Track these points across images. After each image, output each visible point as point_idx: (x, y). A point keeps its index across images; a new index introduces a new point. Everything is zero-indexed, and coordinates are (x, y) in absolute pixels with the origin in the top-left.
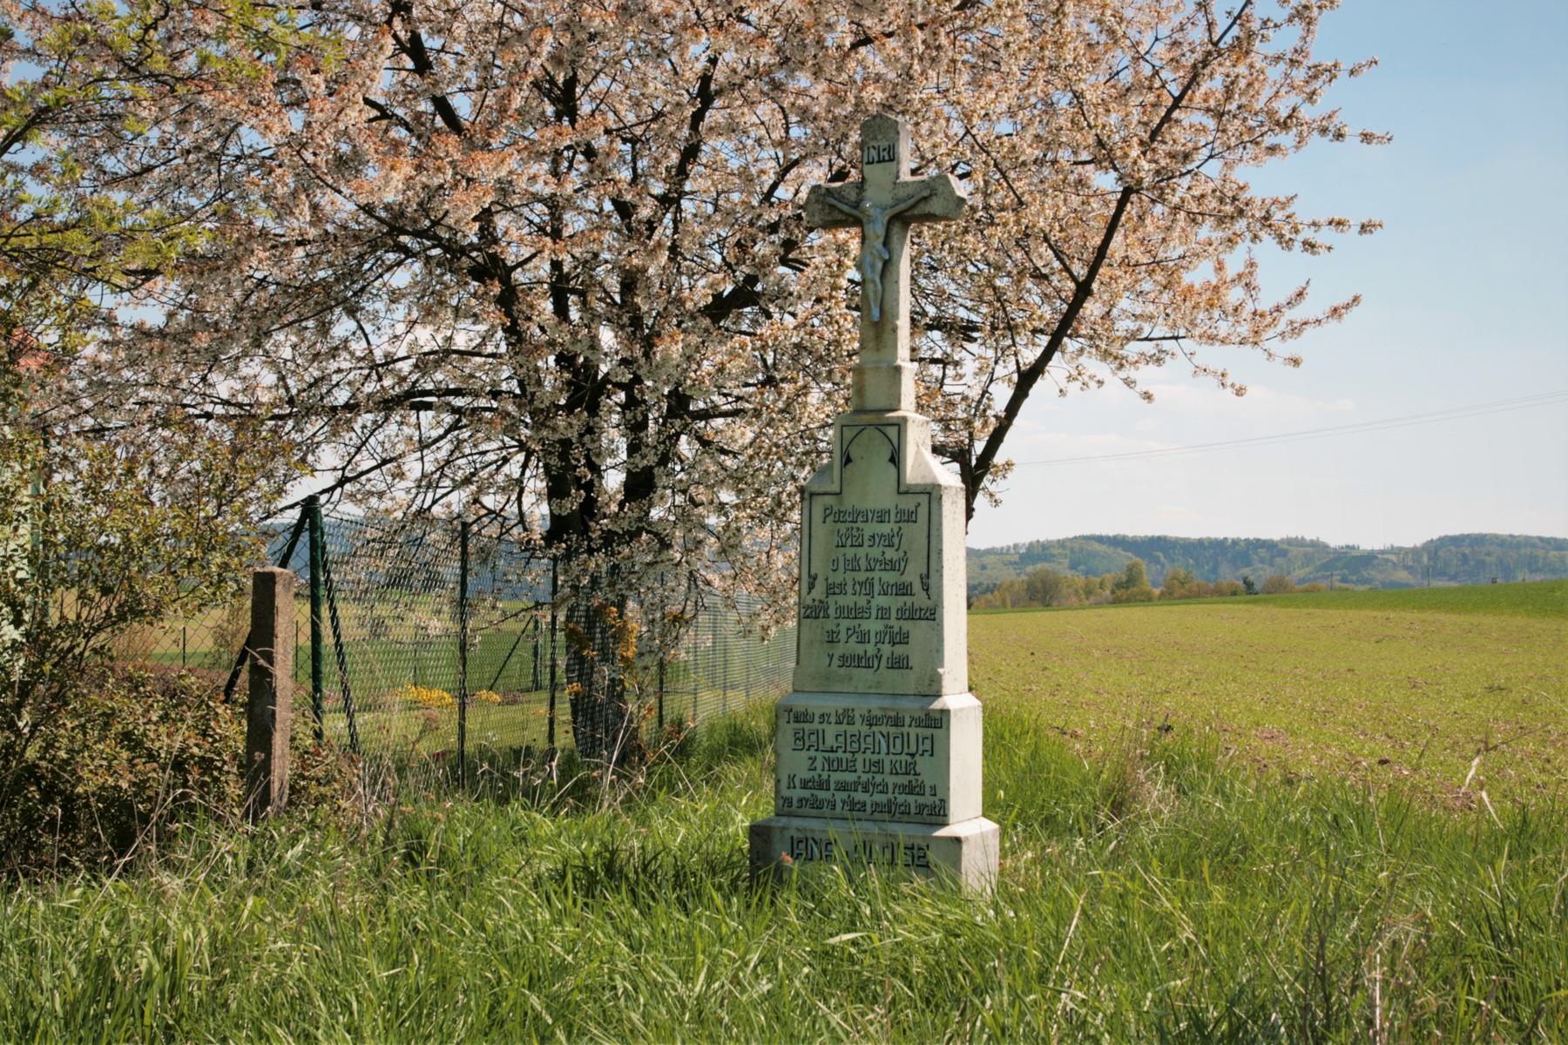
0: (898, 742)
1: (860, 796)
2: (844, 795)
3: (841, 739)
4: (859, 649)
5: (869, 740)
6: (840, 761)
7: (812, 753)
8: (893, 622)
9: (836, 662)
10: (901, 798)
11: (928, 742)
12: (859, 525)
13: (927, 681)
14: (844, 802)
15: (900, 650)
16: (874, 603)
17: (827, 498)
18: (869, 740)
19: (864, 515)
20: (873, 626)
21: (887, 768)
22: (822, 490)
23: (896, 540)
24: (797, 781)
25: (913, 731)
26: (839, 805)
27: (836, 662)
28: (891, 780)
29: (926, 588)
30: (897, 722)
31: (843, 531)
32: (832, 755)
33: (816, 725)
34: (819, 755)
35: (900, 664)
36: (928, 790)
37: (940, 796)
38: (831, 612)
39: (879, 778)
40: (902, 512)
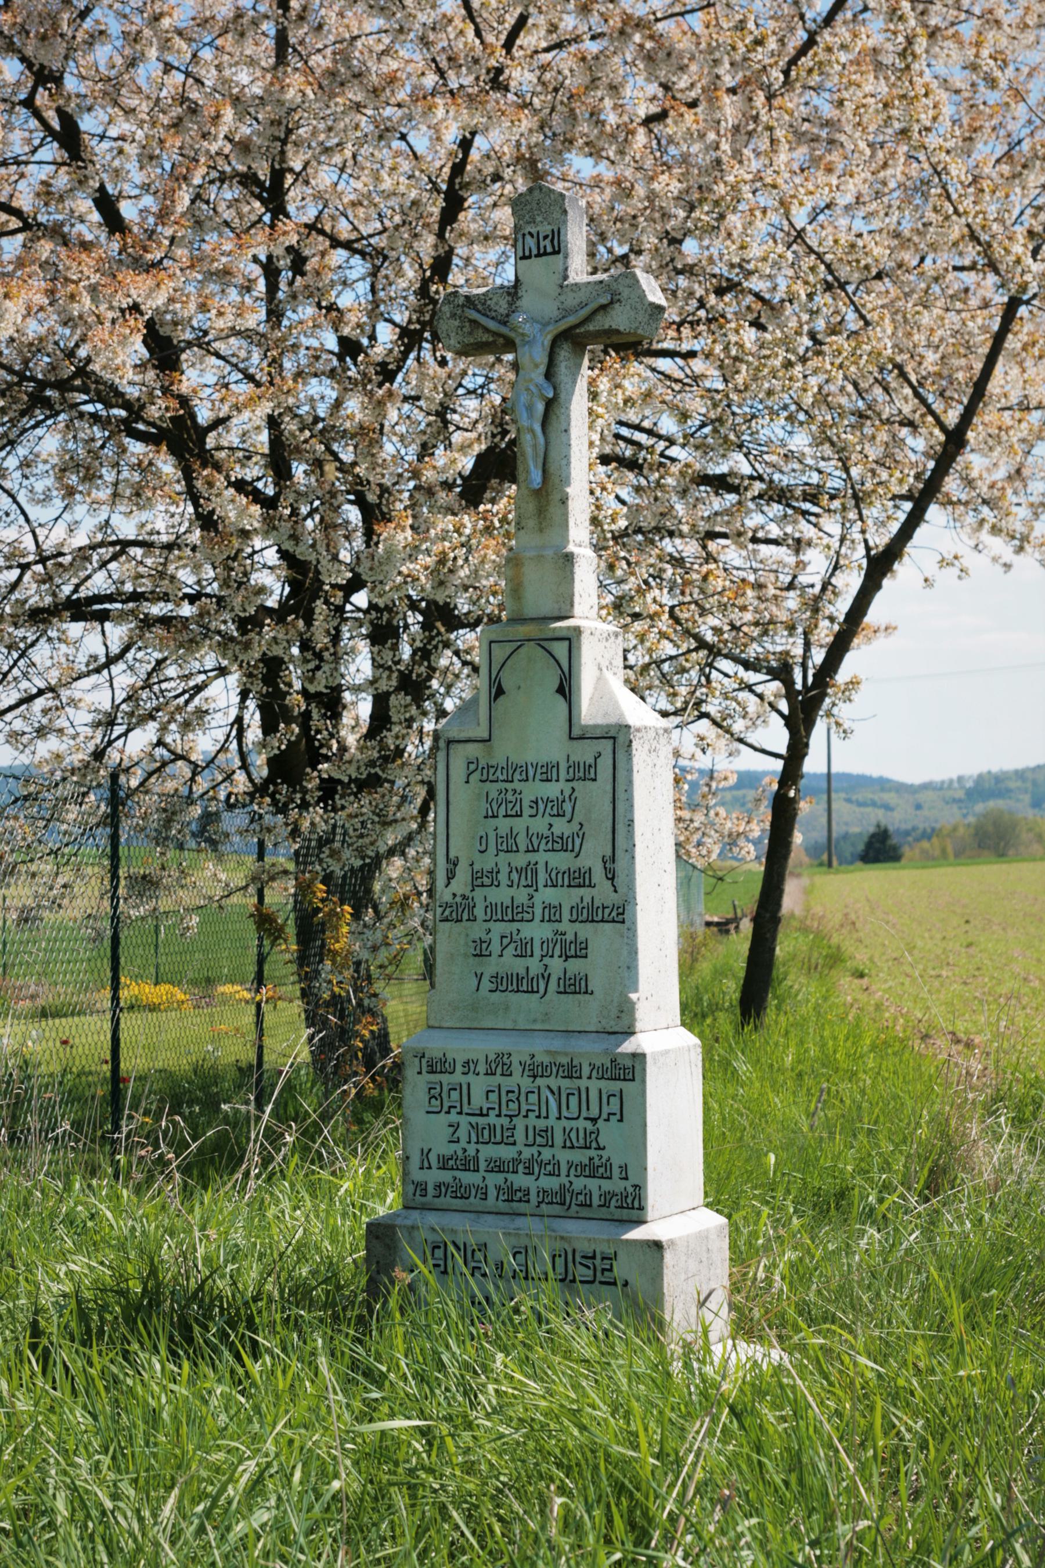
0: (574, 1101)
1: (520, 1180)
2: (498, 1179)
3: (493, 1097)
4: (518, 966)
5: (533, 1098)
6: (492, 1129)
7: (453, 1117)
8: (565, 926)
9: (486, 985)
10: (579, 1183)
11: (615, 1101)
12: (517, 785)
13: (614, 1012)
14: (498, 1189)
15: (575, 966)
16: (538, 899)
17: (470, 746)
18: (533, 1098)
19: (522, 771)
20: (537, 931)
21: (559, 1139)
22: (463, 736)
23: (567, 807)
24: (433, 1158)
25: (594, 1085)
26: (492, 1193)
27: (486, 985)
28: (564, 1157)
29: (611, 877)
30: (571, 1072)
31: (493, 795)
32: (482, 1121)
33: (458, 1077)
34: (464, 1120)
35: (575, 987)
36: (616, 1172)
37: (633, 1180)
38: (479, 912)
39: (547, 1154)
40: (576, 766)
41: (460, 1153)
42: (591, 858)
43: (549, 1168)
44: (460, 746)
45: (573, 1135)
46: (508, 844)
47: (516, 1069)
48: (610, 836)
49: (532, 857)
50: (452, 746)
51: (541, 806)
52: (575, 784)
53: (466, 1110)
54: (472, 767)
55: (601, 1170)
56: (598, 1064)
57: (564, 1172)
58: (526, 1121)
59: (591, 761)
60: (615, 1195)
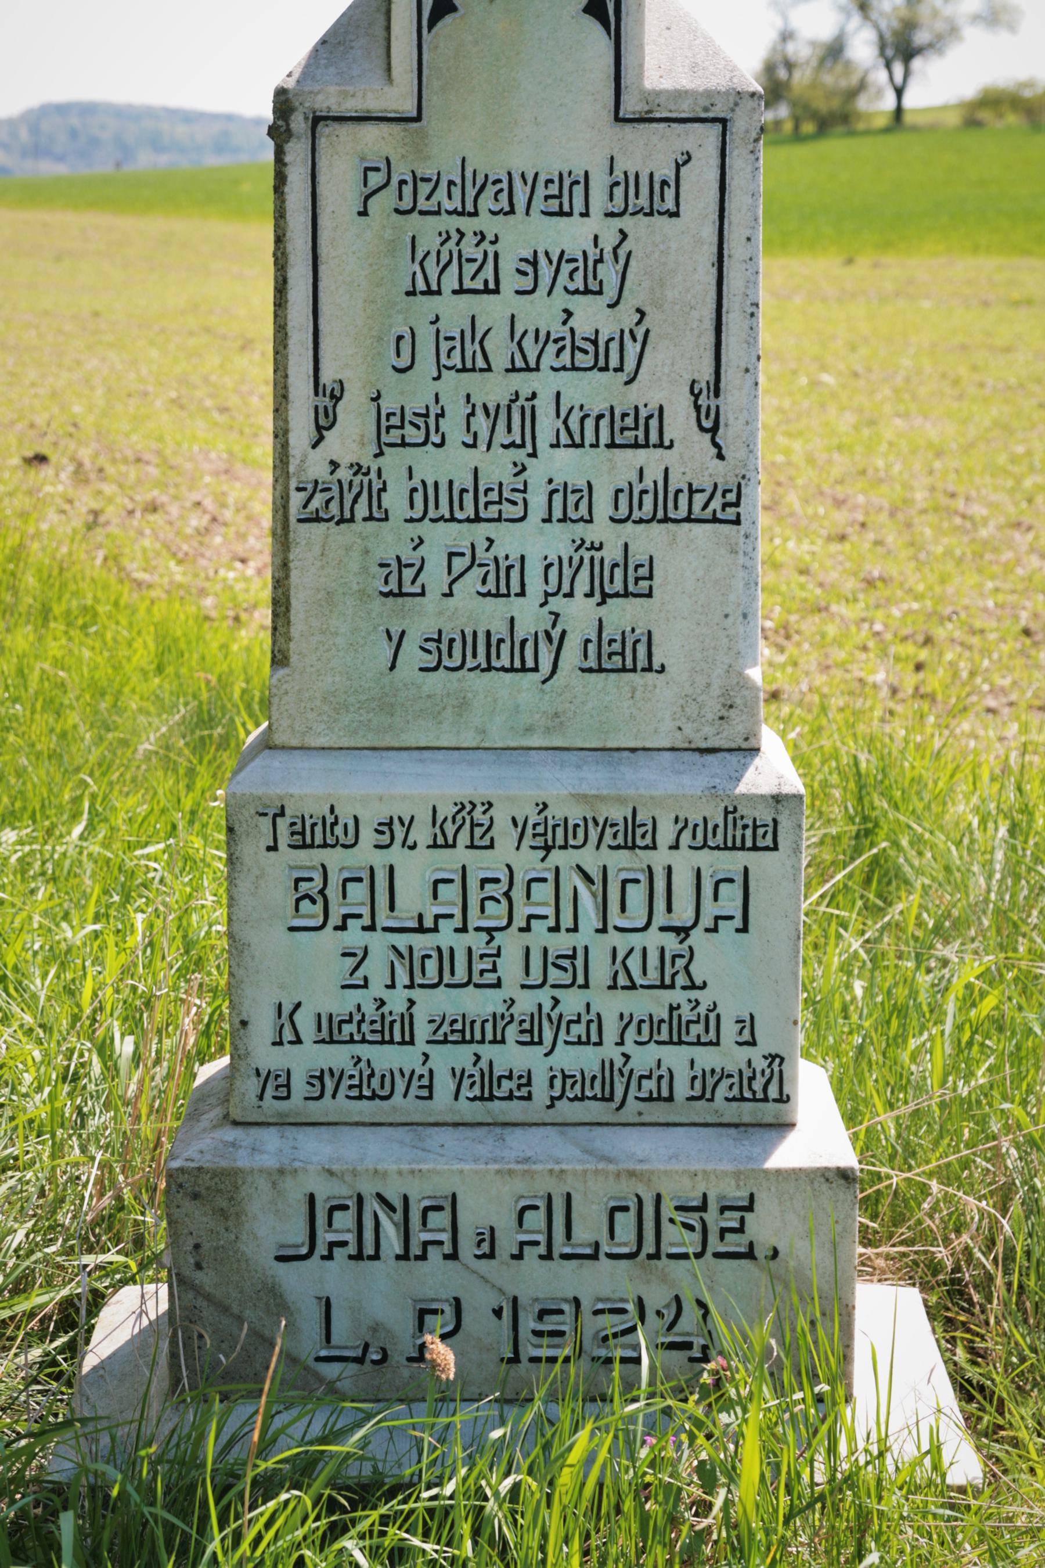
0: (636, 895)
1: (511, 1056)
2: (462, 1056)
3: (450, 893)
4: (492, 616)
5: (543, 892)
6: (446, 958)
7: (354, 936)
8: (600, 530)
9: (412, 655)
10: (644, 1058)
11: (731, 894)
12: (484, 222)
13: (713, 708)
14: (459, 1076)
15: (621, 615)
16: (537, 473)
17: (371, 133)
18: (543, 892)
19: (507, 193)
20: (536, 542)
21: (601, 970)
22: (351, 106)
23: (609, 273)
24: (305, 1022)
25: (684, 863)
26: (444, 1085)
27: (412, 655)
28: (613, 1007)
29: (712, 427)
30: (634, 835)
31: (428, 242)
32: (421, 942)
33: (365, 854)
34: (379, 943)
35: (625, 657)
36: (729, 1031)
37: (767, 1044)
38: (395, 500)
39: (572, 1002)
40: (630, 182)
41: (370, 1010)
42: (664, 384)
43: (578, 1030)
44: (344, 131)
45: (634, 964)
46: (468, 354)
47: (505, 835)
48: (710, 338)
49: (524, 383)
50: (325, 130)
51: (546, 272)
52: (626, 223)
53: (383, 919)
54: (376, 179)
55: (696, 1029)
56: (695, 818)
57: (611, 1033)
58: (527, 938)
59: (670, 174)
60: (725, 1075)
